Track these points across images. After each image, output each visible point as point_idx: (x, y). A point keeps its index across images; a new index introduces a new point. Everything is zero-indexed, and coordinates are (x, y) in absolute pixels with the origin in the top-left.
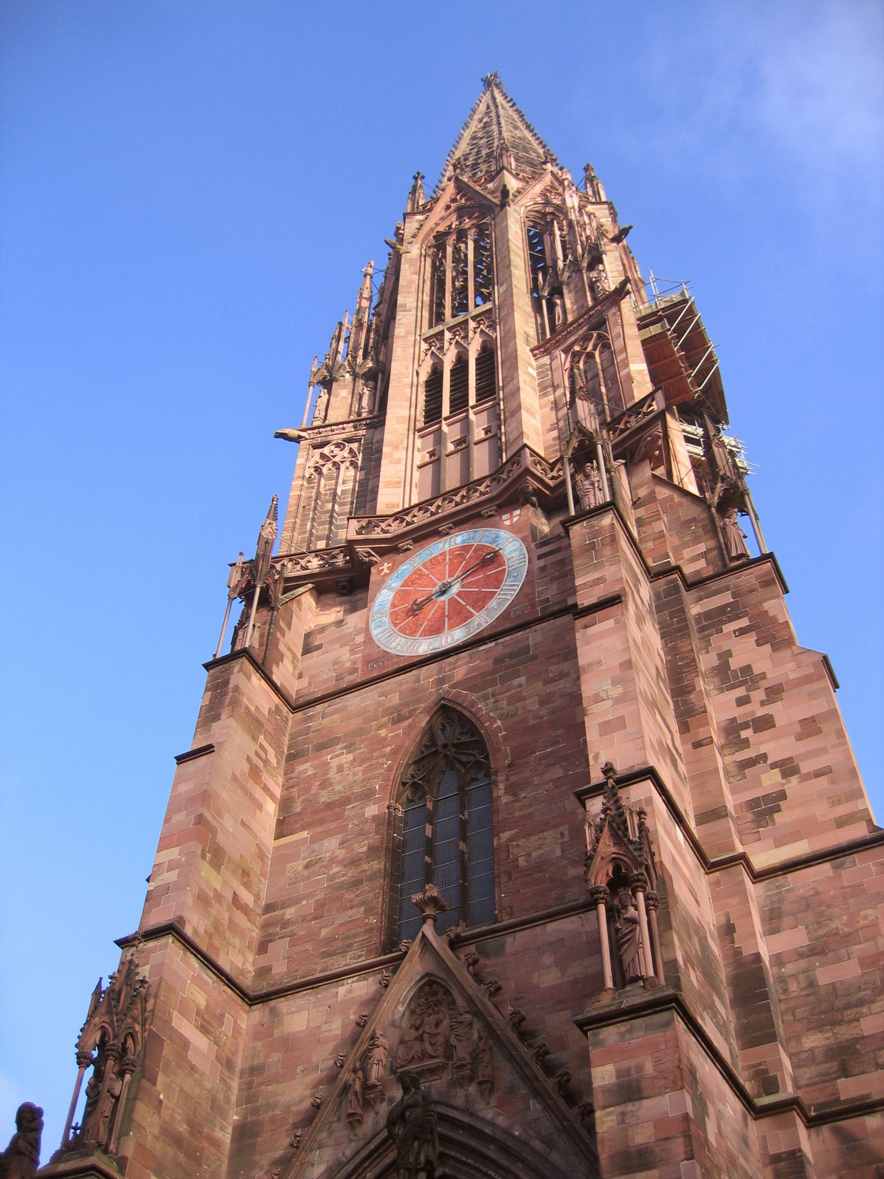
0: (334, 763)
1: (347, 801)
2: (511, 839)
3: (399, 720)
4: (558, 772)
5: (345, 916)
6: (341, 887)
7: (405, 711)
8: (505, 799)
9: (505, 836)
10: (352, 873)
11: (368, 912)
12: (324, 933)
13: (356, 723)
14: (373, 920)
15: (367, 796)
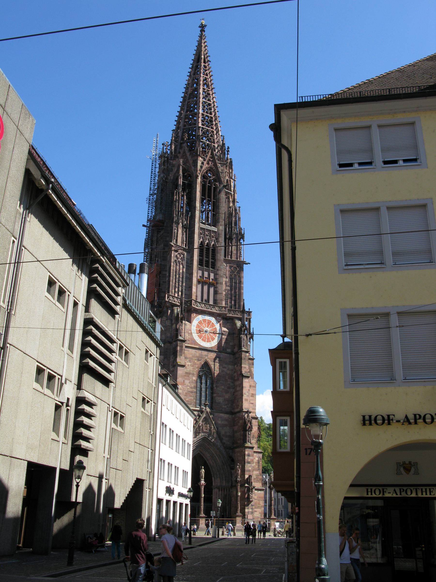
0: (187, 363)
1: (190, 374)
2: (216, 396)
3: (198, 360)
4: (223, 387)
5: (191, 398)
6: (189, 391)
7: (200, 359)
8: (215, 388)
9: (215, 395)
10: (191, 390)
11: (194, 399)
12: (187, 399)
13: (191, 356)
14: (195, 401)
15: (193, 374)
